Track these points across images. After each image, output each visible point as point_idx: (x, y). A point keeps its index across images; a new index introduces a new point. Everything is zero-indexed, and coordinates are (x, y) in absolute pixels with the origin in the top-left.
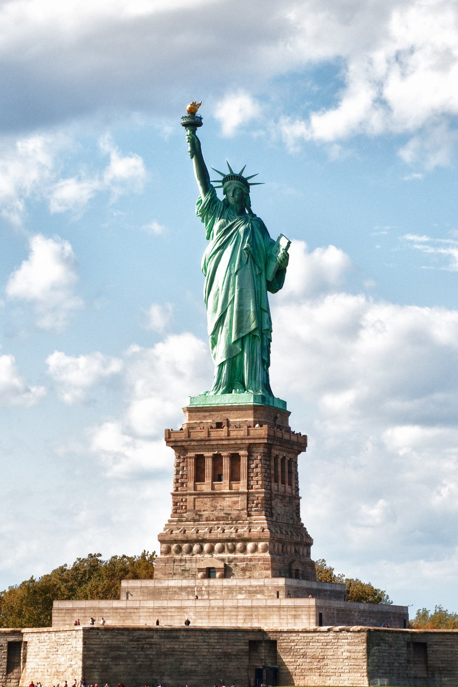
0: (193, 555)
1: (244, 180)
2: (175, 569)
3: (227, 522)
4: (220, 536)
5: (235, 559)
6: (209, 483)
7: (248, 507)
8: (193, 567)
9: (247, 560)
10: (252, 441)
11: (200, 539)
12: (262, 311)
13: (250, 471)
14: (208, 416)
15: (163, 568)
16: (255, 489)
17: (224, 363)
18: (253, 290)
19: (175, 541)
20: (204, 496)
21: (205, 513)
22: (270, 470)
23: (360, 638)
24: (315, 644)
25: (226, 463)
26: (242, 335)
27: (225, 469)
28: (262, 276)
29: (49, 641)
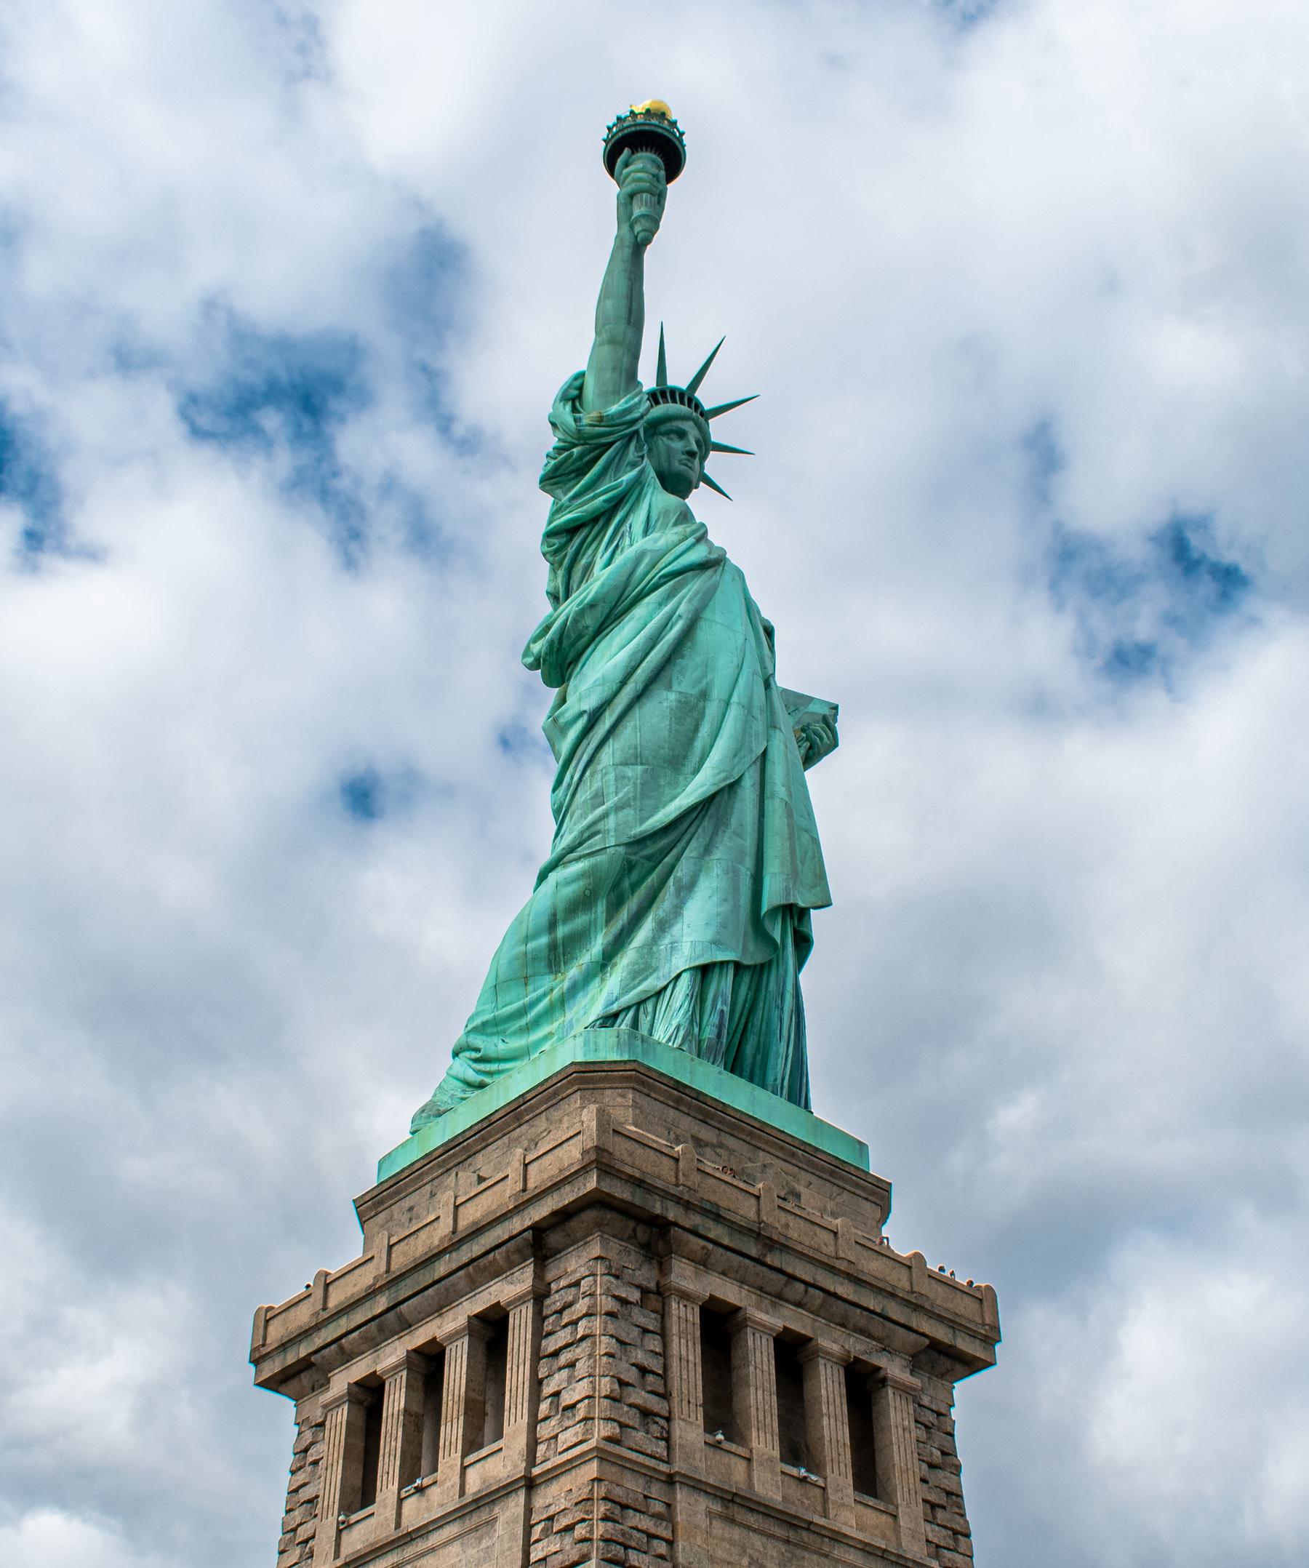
6: (770, 1460)
10: (941, 1333)
14: (714, 1146)
17: (717, 970)
20: (751, 1519)
27: (832, 1420)
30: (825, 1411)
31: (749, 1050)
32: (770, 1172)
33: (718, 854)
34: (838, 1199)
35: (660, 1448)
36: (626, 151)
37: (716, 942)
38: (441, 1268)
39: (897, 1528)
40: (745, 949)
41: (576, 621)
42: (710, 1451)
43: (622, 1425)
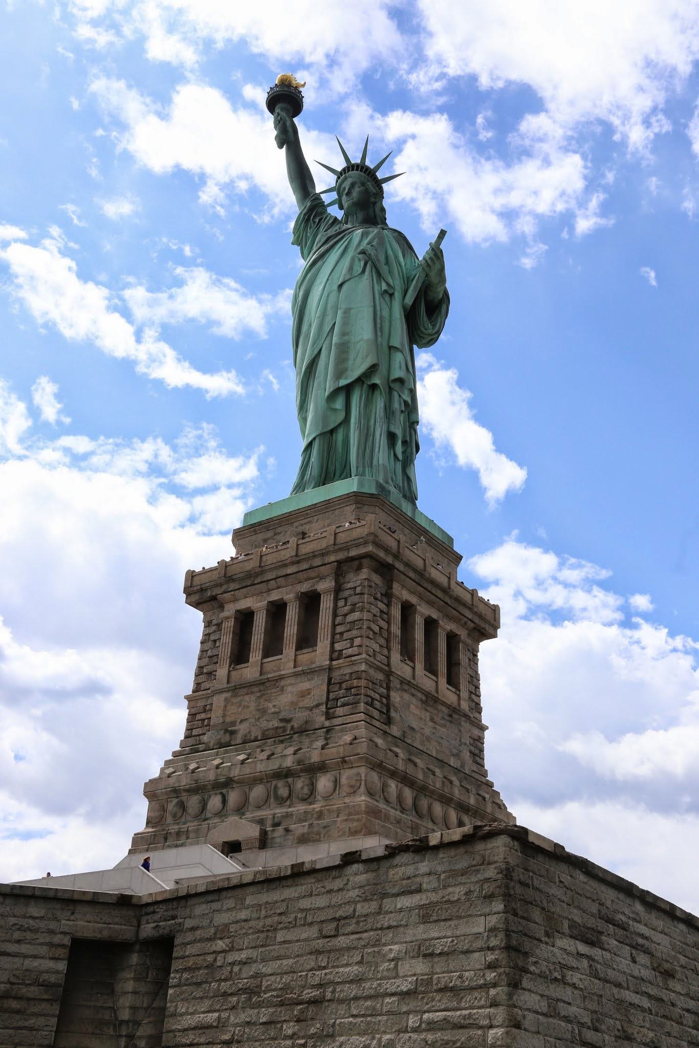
0: (205, 820)
1: (370, 172)
4: (261, 767)
5: (288, 816)
9: (313, 815)
10: (341, 556)
12: (392, 351)
13: (339, 619)
14: (272, 538)
16: (345, 658)
18: (371, 309)
19: (176, 791)
22: (389, 623)
23: (474, 879)
24: (291, 935)
26: (343, 382)
28: (395, 298)
34: (333, 515)
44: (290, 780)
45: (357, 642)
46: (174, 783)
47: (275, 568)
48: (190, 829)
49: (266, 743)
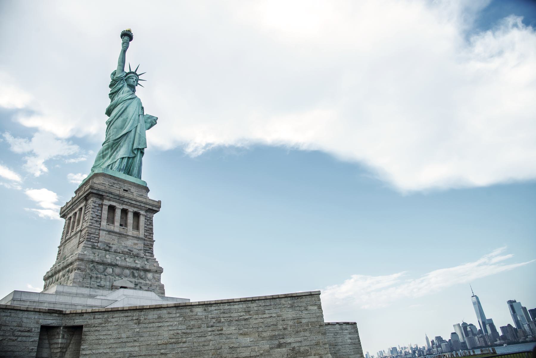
2: (91, 284)
3: (131, 256)
4: (128, 264)
5: (140, 283)
6: (118, 226)
7: (144, 250)
8: (107, 285)
10: (150, 207)
11: (114, 264)
14: (117, 184)
15: (81, 282)
17: (125, 158)
19: (92, 262)
20: (113, 234)
21: (113, 246)
25: (130, 216)
26: (140, 148)
29: (181, 319)
30: (129, 219)
31: (131, 169)
32: (125, 187)
33: (126, 141)
35: (99, 226)
36: (123, 36)
37: (124, 154)
38: (77, 202)
39: (139, 234)
40: (130, 155)
41: (110, 108)
42: (107, 226)
43: (92, 223)
44: (137, 271)
45: (151, 235)
46: (92, 259)
47: (128, 199)
48: (102, 277)
49: (125, 256)
